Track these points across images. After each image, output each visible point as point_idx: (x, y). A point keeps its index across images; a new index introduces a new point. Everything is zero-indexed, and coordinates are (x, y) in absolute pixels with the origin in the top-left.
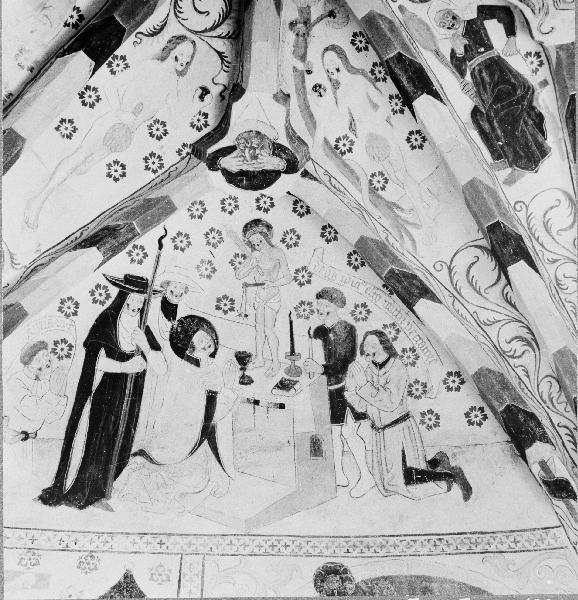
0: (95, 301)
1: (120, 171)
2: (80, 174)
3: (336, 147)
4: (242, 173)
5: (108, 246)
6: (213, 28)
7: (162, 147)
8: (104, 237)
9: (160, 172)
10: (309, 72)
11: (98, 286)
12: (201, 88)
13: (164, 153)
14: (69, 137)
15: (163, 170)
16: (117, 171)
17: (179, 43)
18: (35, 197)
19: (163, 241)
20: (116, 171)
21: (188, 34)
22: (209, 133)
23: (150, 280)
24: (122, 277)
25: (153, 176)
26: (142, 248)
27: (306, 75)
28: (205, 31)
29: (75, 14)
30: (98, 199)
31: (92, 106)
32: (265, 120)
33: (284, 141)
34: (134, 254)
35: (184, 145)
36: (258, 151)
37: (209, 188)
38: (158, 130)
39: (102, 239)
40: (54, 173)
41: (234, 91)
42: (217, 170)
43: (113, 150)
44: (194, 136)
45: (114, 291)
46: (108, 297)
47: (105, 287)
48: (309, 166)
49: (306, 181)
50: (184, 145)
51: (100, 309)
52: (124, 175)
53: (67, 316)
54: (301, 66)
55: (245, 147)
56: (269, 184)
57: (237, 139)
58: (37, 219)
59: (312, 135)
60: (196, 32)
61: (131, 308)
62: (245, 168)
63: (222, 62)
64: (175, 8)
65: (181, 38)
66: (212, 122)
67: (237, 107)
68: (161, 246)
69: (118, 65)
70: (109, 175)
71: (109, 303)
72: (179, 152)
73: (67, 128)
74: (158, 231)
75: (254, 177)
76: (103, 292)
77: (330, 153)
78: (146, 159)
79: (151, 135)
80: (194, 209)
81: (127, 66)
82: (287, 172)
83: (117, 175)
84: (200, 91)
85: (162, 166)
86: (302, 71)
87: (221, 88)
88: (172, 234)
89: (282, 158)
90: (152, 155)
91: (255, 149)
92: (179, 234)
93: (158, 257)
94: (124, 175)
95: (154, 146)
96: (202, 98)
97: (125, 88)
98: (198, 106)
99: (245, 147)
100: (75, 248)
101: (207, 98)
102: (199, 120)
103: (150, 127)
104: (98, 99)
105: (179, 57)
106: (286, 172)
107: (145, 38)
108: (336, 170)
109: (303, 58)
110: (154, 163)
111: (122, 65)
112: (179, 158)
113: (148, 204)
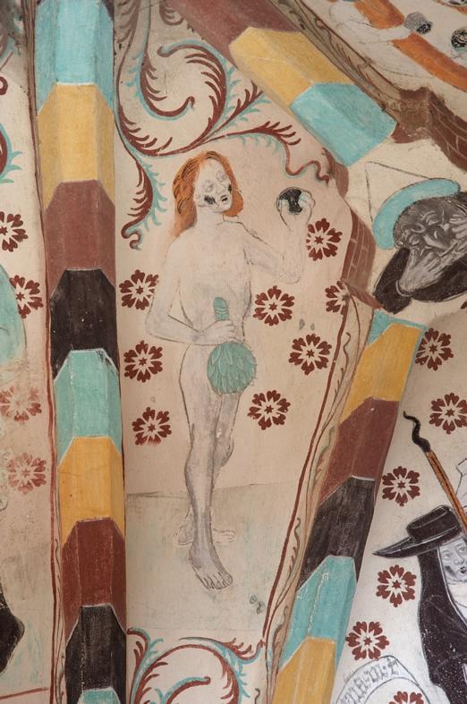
0: (396, 601)
1: (275, 405)
2: (225, 460)
4: (449, 272)
5: (344, 537)
6: (219, 107)
7: (302, 323)
8: (335, 529)
9: (330, 357)
10: (426, 28)
11: (383, 577)
12: (281, 197)
13: (313, 327)
14: (166, 431)
15: (332, 351)
16: (272, 410)
17: (192, 180)
18: (196, 538)
19: (422, 435)
20: (269, 410)
21: (192, 154)
22: (350, 244)
23: (448, 503)
24: (403, 535)
25: (325, 372)
26: (400, 471)
27: (427, 37)
28: (211, 123)
29: (19, 289)
30: (275, 475)
31: (157, 368)
32: (415, 180)
34: (396, 490)
35: (330, 292)
36: (446, 227)
38: (275, 306)
39: (327, 537)
40: (191, 493)
41: (334, 172)
42: (406, 303)
43: (237, 392)
44: (336, 263)
45: (412, 565)
46: (409, 579)
47: (396, 570)
50: (330, 292)
51: (411, 608)
52: (284, 405)
53: (375, 655)
54: (401, 32)
55: (421, 237)
57: (396, 236)
58: (221, 569)
60: (201, 140)
61: (456, 568)
62: (447, 261)
63: (279, 137)
64: (139, 147)
65: (189, 171)
68: (424, 445)
69: (140, 291)
70: (265, 424)
71: (418, 587)
72: (332, 307)
73: (151, 426)
74: (403, 429)
76: (396, 578)
78: (295, 358)
79: (272, 321)
80: (427, 353)
81: (153, 280)
83: (275, 414)
84: (285, 203)
85: (325, 347)
86: (412, 37)
87: (311, 170)
88: (424, 415)
90: (298, 344)
91: (437, 227)
92: (437, 405)
93: (434, 462)
94: (284, 405)
95: (287, 332)
96: (295, 208)
97: (177, 307)
98: (300, 223)
100: (304, 577)
101: (303, 201)
102: (319, 240)
103: (259, 314)
104: (157, 352)
105: (211, 195)
107: (141, 227)
109: (395, 18)
110: (311, 353)
111: (145, 285)
112: (338, 316)
113: (347, 431)
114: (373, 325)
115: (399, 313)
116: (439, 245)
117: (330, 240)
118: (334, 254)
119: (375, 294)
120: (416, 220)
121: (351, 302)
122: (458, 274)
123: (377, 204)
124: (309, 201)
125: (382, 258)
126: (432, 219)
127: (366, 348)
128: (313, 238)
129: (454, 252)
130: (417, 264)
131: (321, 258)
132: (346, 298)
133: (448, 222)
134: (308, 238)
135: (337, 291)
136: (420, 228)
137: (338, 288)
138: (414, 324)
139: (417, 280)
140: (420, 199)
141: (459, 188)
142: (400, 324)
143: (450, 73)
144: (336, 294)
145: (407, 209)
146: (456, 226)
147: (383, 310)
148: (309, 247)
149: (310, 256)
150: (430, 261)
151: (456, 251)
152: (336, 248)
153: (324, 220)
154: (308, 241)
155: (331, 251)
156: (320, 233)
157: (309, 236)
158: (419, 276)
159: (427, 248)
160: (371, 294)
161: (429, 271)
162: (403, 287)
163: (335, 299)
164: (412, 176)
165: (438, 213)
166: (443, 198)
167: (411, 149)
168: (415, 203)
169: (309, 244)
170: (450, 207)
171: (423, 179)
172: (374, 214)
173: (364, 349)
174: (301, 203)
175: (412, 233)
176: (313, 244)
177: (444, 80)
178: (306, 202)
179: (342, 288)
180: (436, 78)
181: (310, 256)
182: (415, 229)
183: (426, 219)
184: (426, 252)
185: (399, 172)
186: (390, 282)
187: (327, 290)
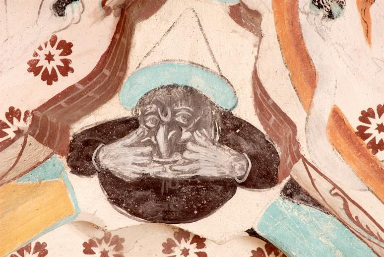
3: (362, 133)
4: (149, 184)
22: (72, 88)
32: (213, 67)
33: (247, 112)
35: (12, 113)
36: (186, 135)
37: (64, 212)
42: (88, 173)
44: (46, 92)
48: (299, 172)
49: (288, 207)
50: (12, 113)
55: (159, 123)
56: (204, 210)
57: (142, 103)
59: (308, 106)
62: (153, 170)
66: (84, 63)
67: (145, 33)
75: (172, 193)
77: (344, 144)
82: (250, 183)
89: (240, 151)
98: (50, 25)
99: (159, 123)
102: (49, 58)
106: (245, 185)
108: (360, 184)
114: (40, 168)
115: (75, 176)
116: (163, 148)
117: (59, 67)
118: (50, 83)
119: (76, 137)
120: (170, 105)
121: (21, 140)
122: (148, 193)
123: (155, 58)
124: (77, 15)
125: (112, 110)
126: (184, 117)
127: (13, 183)
128: (46, 51)
129: (167, 166)
130: (131, 146)
131: (36, 74)
132: (19, 132)
133: (192, 132)
134: (43, 46)
135: (19, 118)
136: (166, 115)
137: (22, 117)
138: (75, 200)
139: (116, 161)
140: (195, 87)
141: (234, 107)
142: (66, 187)
143: (286, 22)
144: (15, 119)
145: (175, 86)
146: (195, 142)
147: (64, 160)
148: (36, 55)
149: (30, 63)
150: (142, 154)
151: (170, 168)
152: (56, 80)
153: (70, 45)
154: (40, 48)
155: (49, 78)
156: (56, 53)
157: (46, 45)
158: (122, 160)
159: (153, 139)
160: (71, 134)
161: (133, 164)
162: (101, 155)
163: (9, 124)
164: (210, 57)
165: (194, 115)
166: (212, 104)
167: (235, 31)
168: (186, 87)
169: (38, 52)
170: (209, 119)
171: (216, 70)
172: (145, 64)
173: (9, 182)
174: (69, 9)
175: (156, 113)
176: (42, 55)
177: (276, 23)
178: (73, 12)
179: (25, 120)
180: (273, 15)
181: (30, 63)
182: (162, 112)
183: (180, 110)
184: (149, 143)
185: (205, 44)
186: (97, 138)
187: (11, 109)
